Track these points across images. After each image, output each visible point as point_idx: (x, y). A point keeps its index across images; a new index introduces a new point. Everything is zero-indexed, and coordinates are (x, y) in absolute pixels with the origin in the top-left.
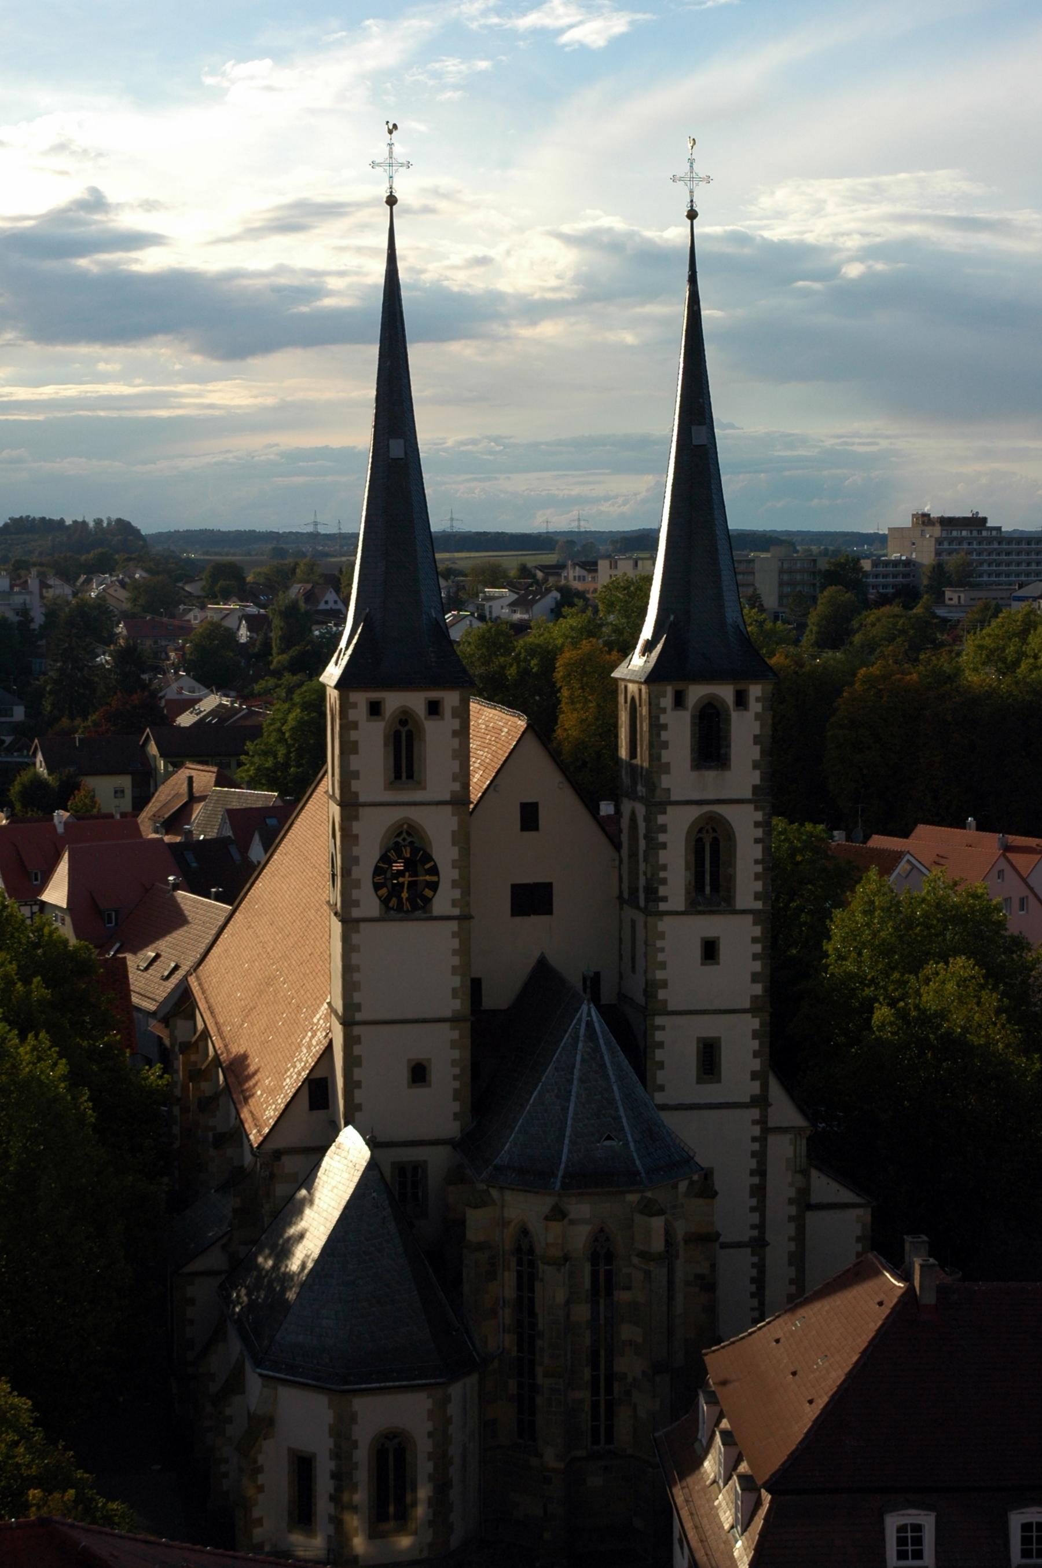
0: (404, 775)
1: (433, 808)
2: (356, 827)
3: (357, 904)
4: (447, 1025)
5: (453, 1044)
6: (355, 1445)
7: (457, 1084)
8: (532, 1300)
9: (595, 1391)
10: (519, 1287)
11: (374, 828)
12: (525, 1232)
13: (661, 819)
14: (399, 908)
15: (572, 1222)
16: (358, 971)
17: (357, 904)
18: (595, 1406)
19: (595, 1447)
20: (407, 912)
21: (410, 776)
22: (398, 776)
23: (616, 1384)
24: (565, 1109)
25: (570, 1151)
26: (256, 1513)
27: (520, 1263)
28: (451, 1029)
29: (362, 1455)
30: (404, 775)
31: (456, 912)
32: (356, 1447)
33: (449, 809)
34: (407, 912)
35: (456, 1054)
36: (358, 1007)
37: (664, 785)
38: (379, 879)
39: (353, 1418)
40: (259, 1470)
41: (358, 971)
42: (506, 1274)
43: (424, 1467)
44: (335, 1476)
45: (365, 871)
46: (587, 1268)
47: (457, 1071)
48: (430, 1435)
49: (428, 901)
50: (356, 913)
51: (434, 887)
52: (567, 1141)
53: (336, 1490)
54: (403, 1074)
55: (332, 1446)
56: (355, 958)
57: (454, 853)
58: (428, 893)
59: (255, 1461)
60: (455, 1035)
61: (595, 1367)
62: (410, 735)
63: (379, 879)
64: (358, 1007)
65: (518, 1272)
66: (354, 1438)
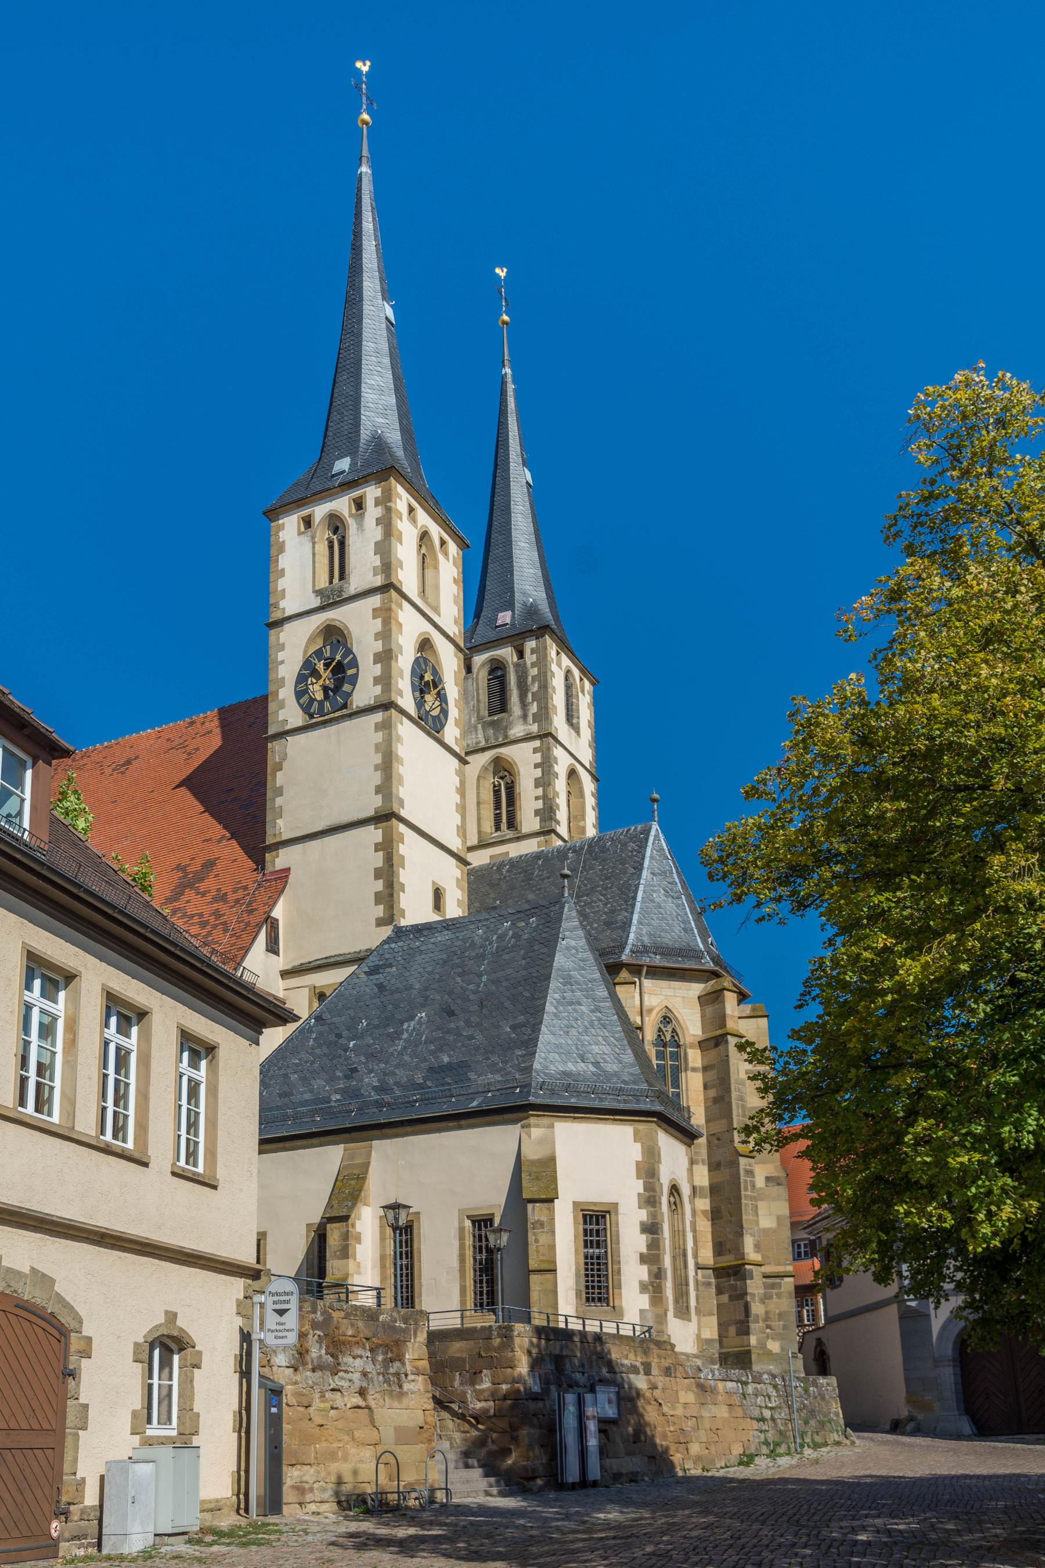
53: (649, 1247)
55: (642, 1191)
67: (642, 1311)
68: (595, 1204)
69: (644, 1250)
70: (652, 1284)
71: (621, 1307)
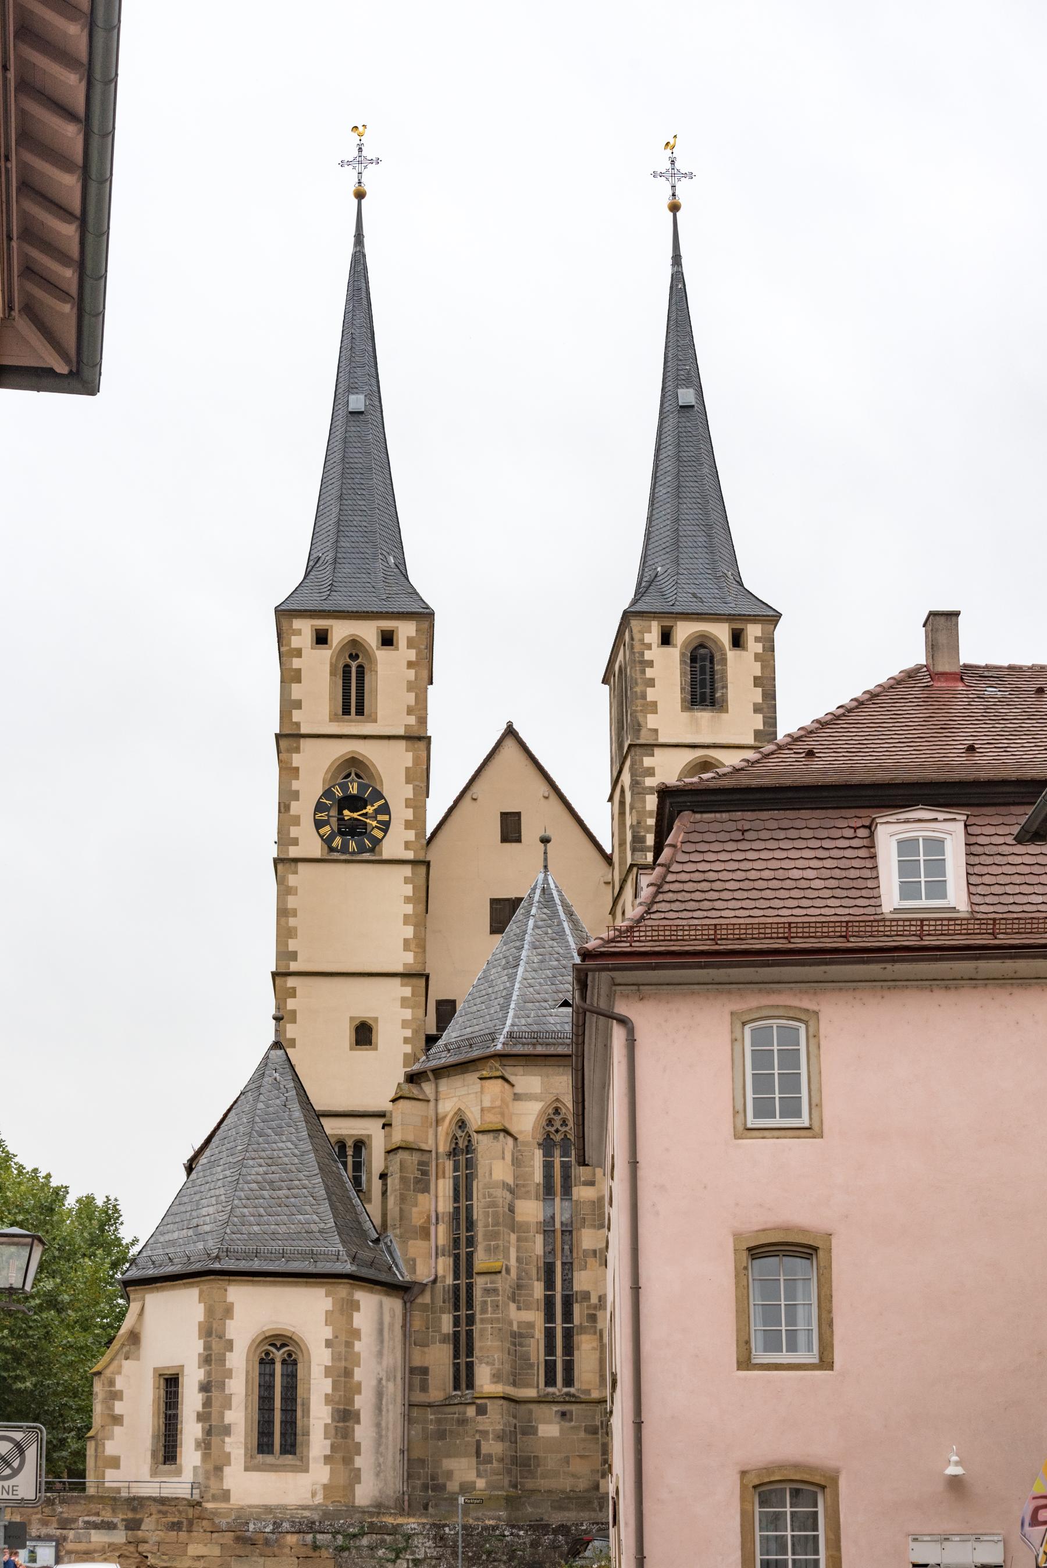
0: (353, 710)
1: (385, 742)
2: (296, 760)
3: (295, 842)
4: (397, 981)
5: (404, 1002)
6: (229, 1345)
7: (408, 1049)
8: (469, 1209)
9: (550, 1317)
10: (456, 1198)
11: (317, 764)
12: (462, 1124)
13: (648, 762)
14: (344, 849)
15: (517, 1097)
16: (295, 916)
17: (295, 842)
18: (550, 1334)
19: (550, 1390)
20: (353, 853)
21: (360, 712)
22: (346, 711)
23: (576, 1308)
24: (512, 978)
25: (516, 1016)
26: (110, 1448)
27: (456, 1169)
28: (402, 985)
29: (239, 1363)
30: (353, 710)
31: (410, 855)
32: (231, 1350)
33: (402, 744)
34: (353, 853)
35: (408, 1014)
36: (294, 956)
37: (650, 726)
38: (322, 816)
39: (228, 1311)
40: (116, 1395)
41: (295, 916)
42: (441, 1182)
44: (205, 1388)
45: (304, 808)
46: (538, 1155)
47: (408, 1033)
48: (328, 1344)
49: (376, 842)
50: (293, 852)
51: (385, 827)
52: (512, 1006)
54: (346, 1034)
55: (201, 1351)
56: (292, 902)
57: (409, 791)
58: (378, 834)
59: (112, 1383)
60: (407, 991)
61: (550, 1284)
62: (361, 671)
63: (322, 816)
64: (294, 956)
65: (456, 1179)
67: (195, 1468)
68: (168, 1368)
69: (200, 1408)
70: (204, 1440)
71: (181, 1466)
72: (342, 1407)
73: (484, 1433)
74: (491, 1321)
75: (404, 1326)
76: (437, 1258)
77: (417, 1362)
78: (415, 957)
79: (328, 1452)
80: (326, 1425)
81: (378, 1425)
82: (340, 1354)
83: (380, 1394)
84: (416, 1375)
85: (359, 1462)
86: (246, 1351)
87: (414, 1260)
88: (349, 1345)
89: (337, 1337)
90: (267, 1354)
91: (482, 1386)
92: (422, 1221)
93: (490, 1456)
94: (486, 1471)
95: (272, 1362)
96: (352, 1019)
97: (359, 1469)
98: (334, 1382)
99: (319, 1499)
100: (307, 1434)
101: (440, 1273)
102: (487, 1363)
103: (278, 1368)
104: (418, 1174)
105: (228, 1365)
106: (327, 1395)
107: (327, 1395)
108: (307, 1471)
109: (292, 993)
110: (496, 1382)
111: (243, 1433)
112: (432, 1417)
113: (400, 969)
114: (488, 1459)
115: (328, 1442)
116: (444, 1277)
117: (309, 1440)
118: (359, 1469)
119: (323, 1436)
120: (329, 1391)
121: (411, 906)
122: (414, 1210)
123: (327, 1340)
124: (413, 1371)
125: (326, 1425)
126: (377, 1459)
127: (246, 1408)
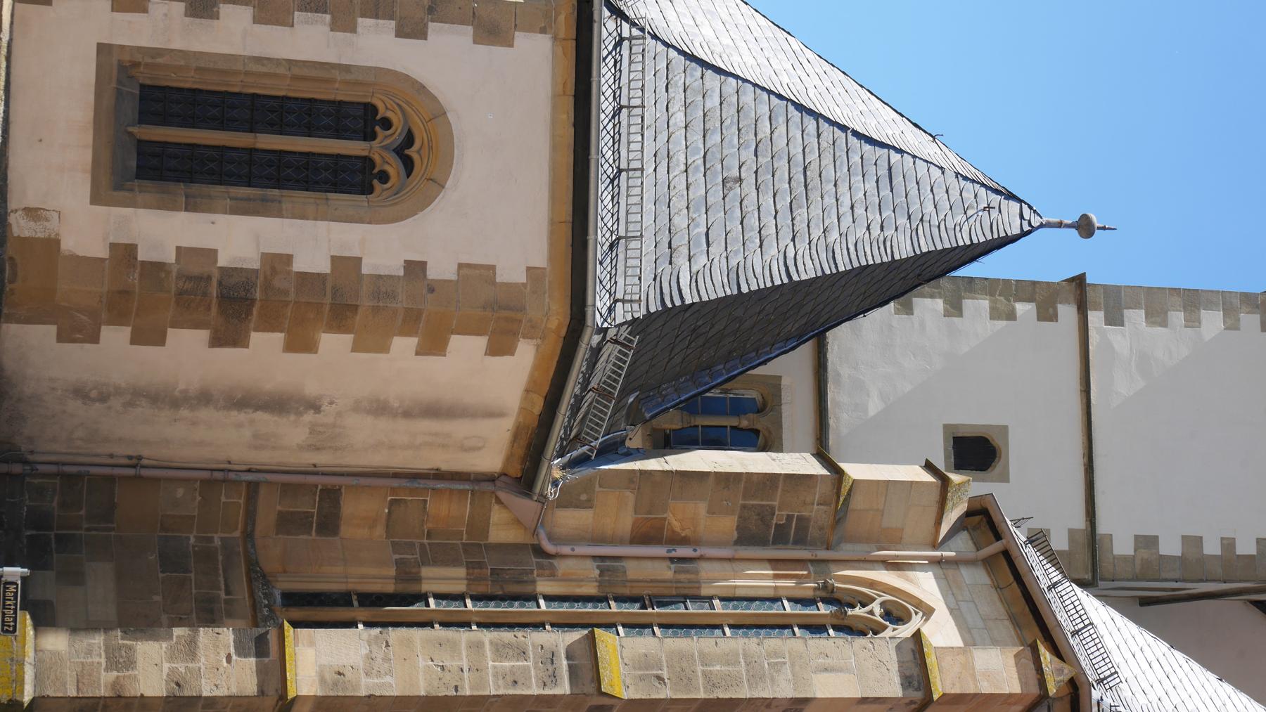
4: (1080, 523)
6: (412, 30)
28: (1071, 532)
32: (400, 33)
36: (1114, 319)
43: (309, 239)
48: (415, 269)
56: (1212, 321)
64: (1114, 319)
66: (432, 26)
72: (258, 295)
73: (191, 650)
74: (477, 669)
75: (438, 475)
76: (594, 558)
77: (351, 507)
78: (1125, 559)
79: (141, 256)
80: (212, 254)
81: (204, 398)
82: (391, 295)
83: (279, 404)
84: (318, 501)
85: (115, 337)
86: (399, 69)
87: (588, 505)
88: (410, 322)
89: (431, 290)
90: (386, 124)
91: (312, 644)
92: (677, 525)
93: (130, 663)
94: (89, 652)
95: (369, 136)
96: (1004, 430)
97: (95, 339)
98: (321, 277)
99: (20, 226)
100: (192, 206)
101: (562, 566)
102: (370, 658)
103: (354, 147)
104: (779, 518)
105: (364, 23)
106: (288, 259)
107: (288, 259)
108: (96, 199)
109: (1047, 314)
110: (322, 680)
111: (196, 47)
112: (217, 542)
113: (1102, 529)
114: (120, 661)
115: (170, 257)
116: (552, 575)
117: (175, 208)
118: (95, 339)
119: (185, 244)
120: (299, 266)
121: (1218, 552)
122: (702, 508)
123: (423, 265)
124: (331, 496)
125: (213, 253)
126: (118, 391)
127: (258, 60)
